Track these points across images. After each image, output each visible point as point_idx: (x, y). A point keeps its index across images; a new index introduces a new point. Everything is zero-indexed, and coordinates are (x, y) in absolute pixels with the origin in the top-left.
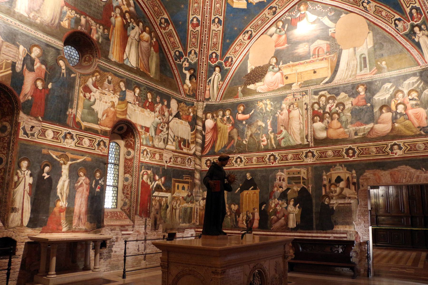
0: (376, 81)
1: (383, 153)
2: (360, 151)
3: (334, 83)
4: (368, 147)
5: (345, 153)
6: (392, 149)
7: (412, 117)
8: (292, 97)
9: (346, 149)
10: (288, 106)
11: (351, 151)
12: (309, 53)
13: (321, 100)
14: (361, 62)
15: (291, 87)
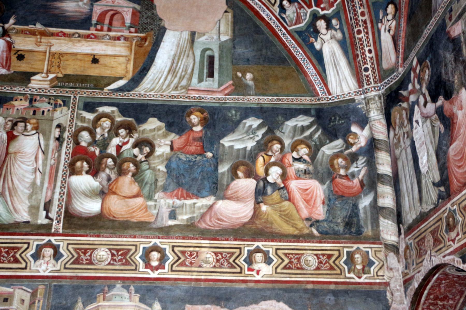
0: (230, 109)
2: (178, 256)
3: (137, 93)
4: (197, 249)
5: (140, 257)
6: (250, 261)
7: (297, 196)
8: (27, 103)
10: (10, 123)
11: (155, 255)
12: (89, 18)
13: (101, 125)
14: (203, 63)
15: (29, 81)
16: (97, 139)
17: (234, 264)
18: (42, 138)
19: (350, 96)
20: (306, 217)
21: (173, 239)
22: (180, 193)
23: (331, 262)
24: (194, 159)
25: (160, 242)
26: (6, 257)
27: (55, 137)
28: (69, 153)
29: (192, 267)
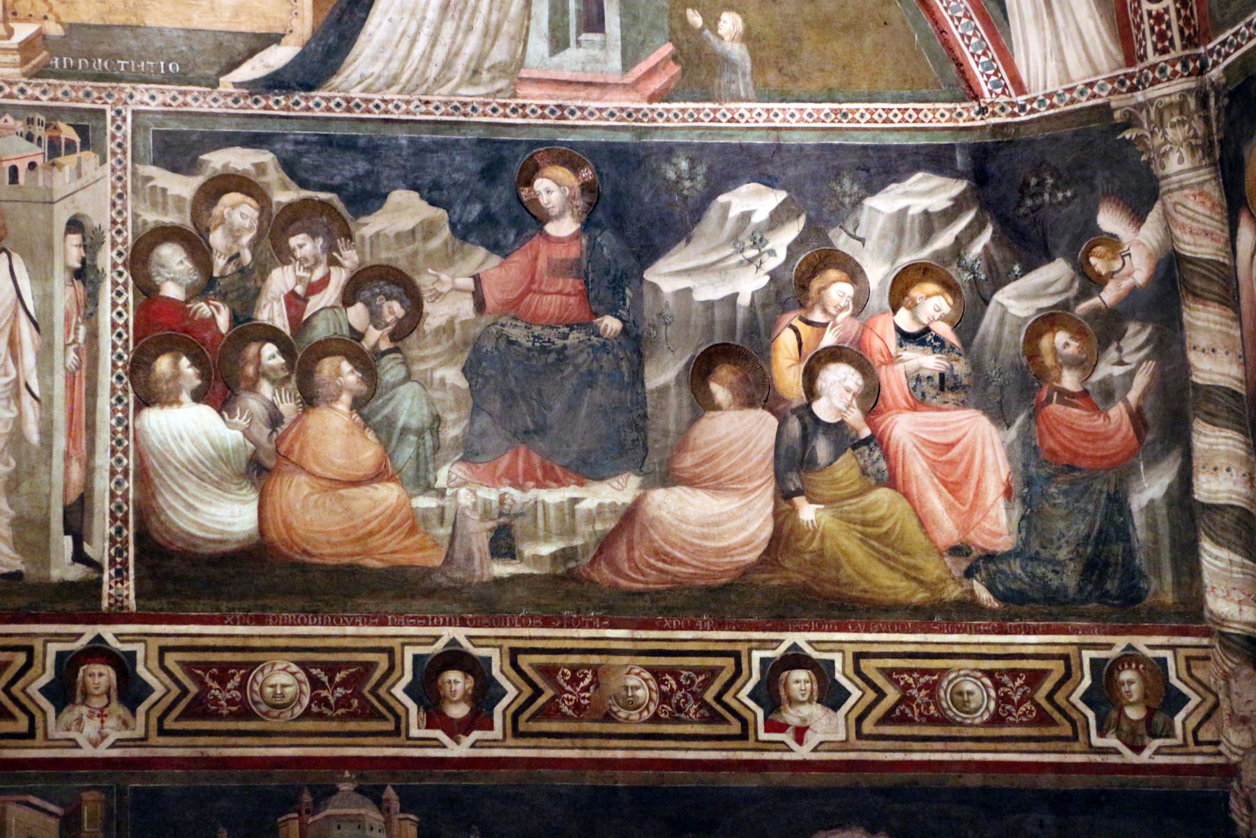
0: (669, 151)
1: (704, 720)
4: (595, 659)
5: (407, 690)
7: (917, 468)
9: (417, 659)
11: (456, 682)
13: (222, 221)
16: (216, 274)
17: (718, 708)
18: (23, 268)
19: (1094, 96)
20: (952, 544)
21: (513, 626)
22: (521, 465)
23: (1041, 696)
24: (560, 343)
25: (469, 638)
27: (67, 268)
28: (126, 325)
29: (580, 720)
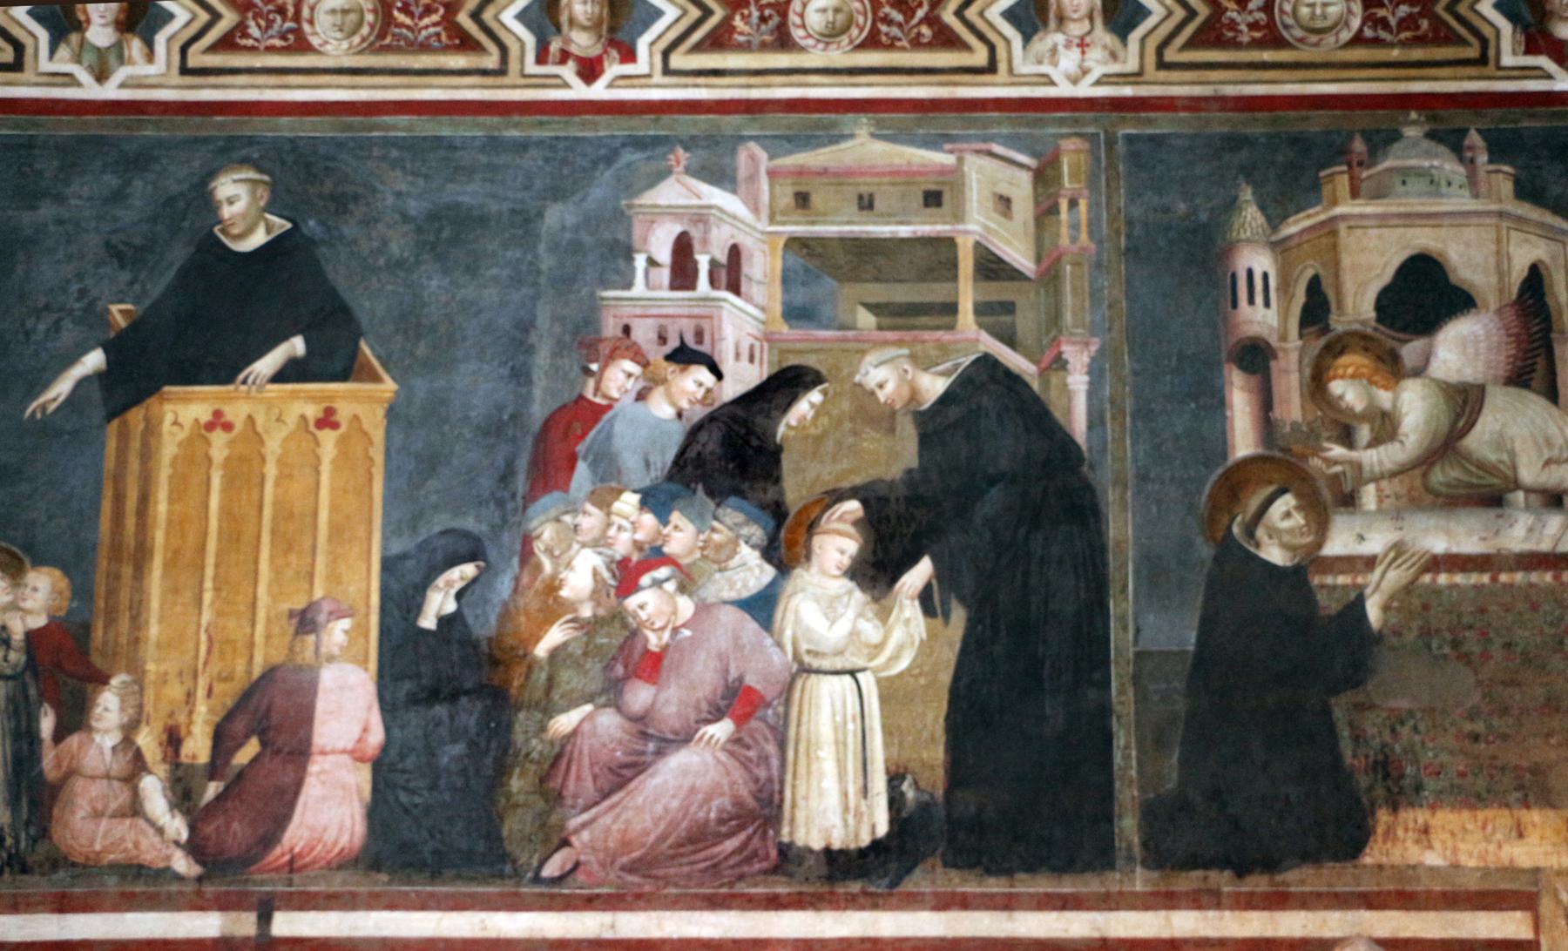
26: (900, 25)
